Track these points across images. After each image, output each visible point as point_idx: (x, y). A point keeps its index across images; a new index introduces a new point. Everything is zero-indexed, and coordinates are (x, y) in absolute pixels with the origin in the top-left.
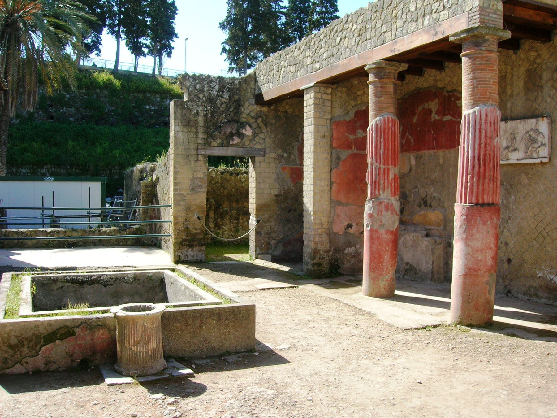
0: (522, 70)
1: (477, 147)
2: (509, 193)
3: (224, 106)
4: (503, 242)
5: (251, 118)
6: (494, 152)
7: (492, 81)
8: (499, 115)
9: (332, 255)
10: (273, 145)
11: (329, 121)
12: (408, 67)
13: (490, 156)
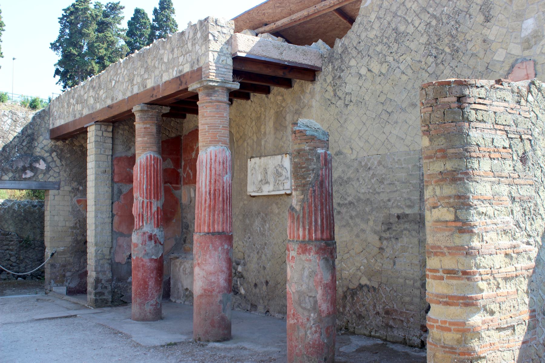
0: (272, 111)
1: (208, 183)
2: (265, 222)
4: (262, 266)
5: (45, 152)
6: (223, 187)
7: (221, 126)
8: (228, 155)
9: (114, 284)
10: (68, 179)
11: (110, 157)
12: (170, 110)
13: (219, 191)
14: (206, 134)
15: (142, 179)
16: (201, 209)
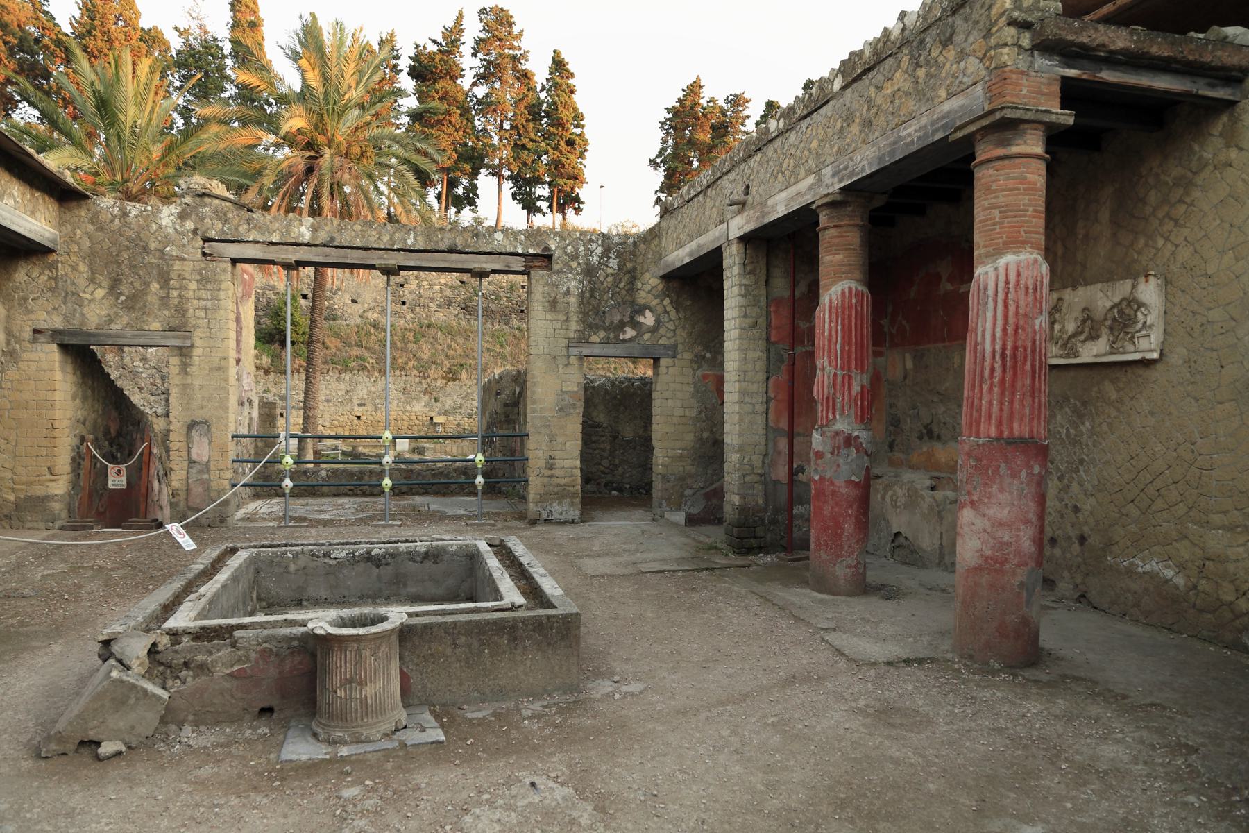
1: (999, 333)
2: (1081, 417)
3: (610, 279)
4: (1070, 505)
6: (1034, 342)
7: (1031, 209)
8: (1044, 273)
13: (1025, 350)
14: (995, 229)
15: (833, 333)
16: (981, 389)
